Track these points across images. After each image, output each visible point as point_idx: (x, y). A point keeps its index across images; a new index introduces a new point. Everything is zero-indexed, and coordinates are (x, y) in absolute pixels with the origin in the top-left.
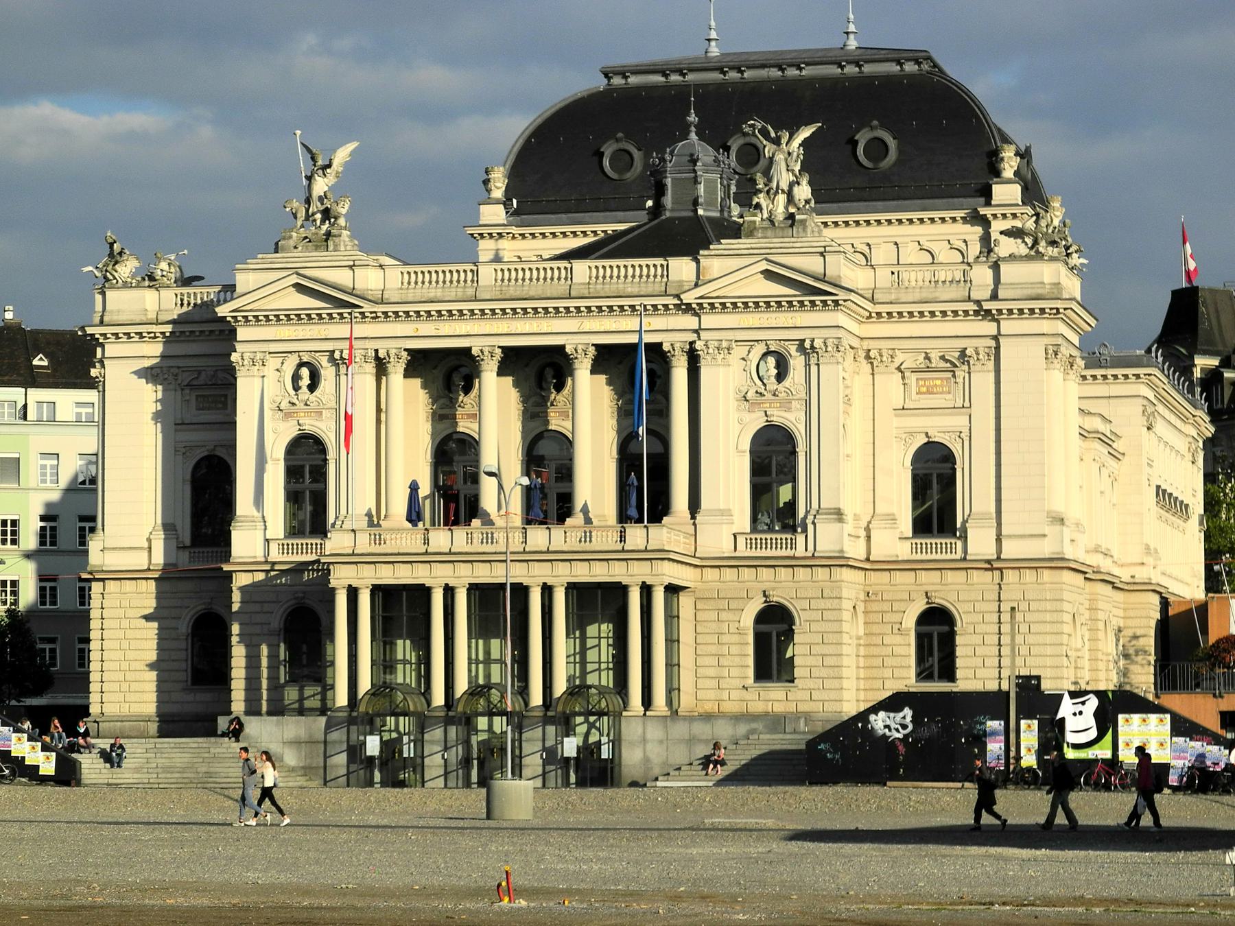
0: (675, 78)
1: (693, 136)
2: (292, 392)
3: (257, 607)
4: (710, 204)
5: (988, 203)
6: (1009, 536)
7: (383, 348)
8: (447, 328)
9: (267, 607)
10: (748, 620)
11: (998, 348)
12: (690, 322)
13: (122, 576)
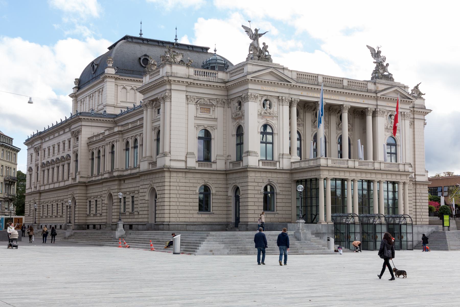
3: (256, 184)
6: (418, 175)
7: (294, 97)
8: (311, 94)
9: (260, 184)
13: (178, 171)
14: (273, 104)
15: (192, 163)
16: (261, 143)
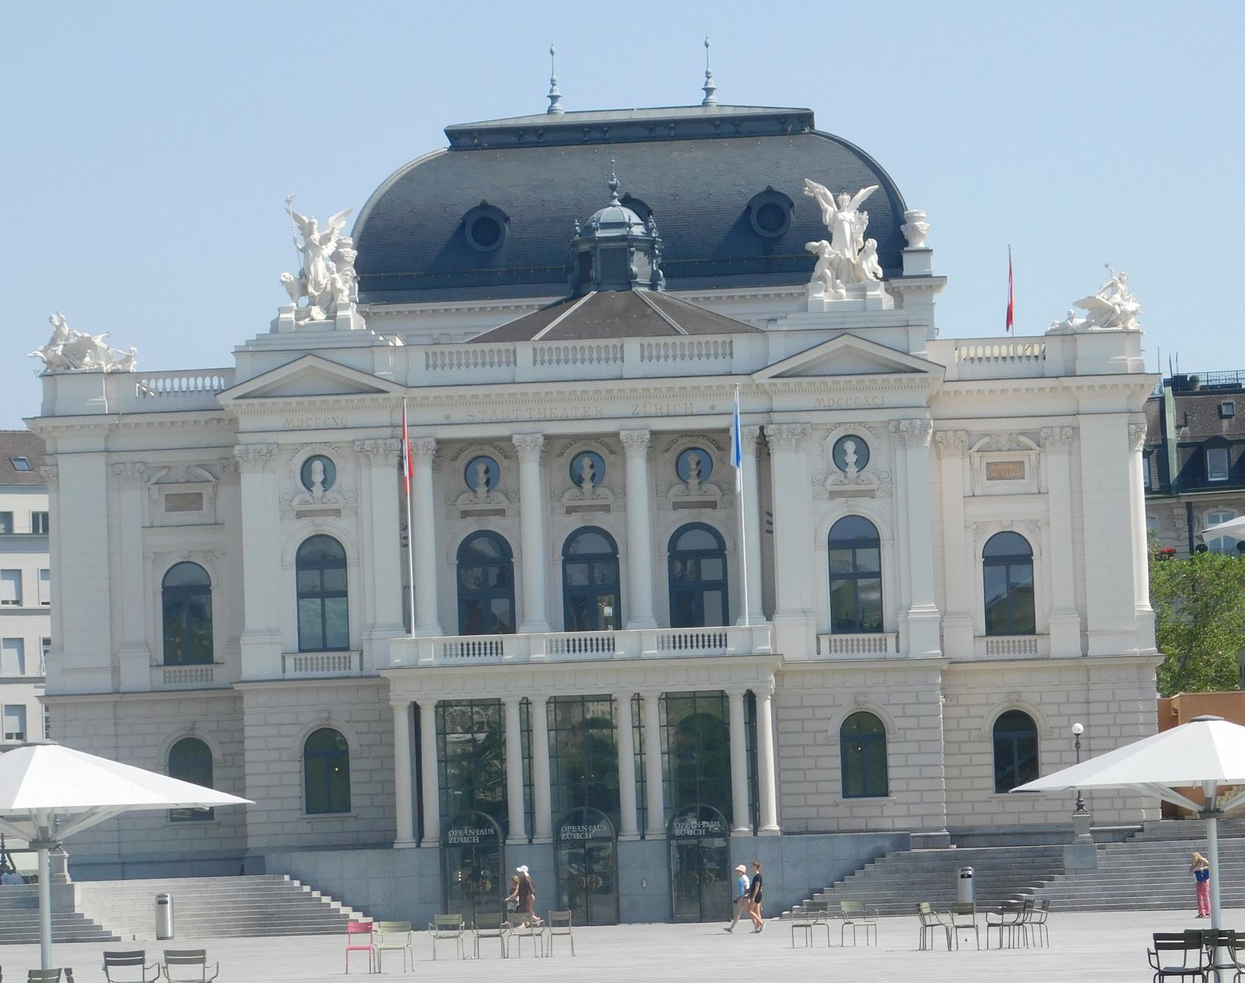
1: (616, 202)
2: (303, 488)
10: (834, 728)
11: (1076, 430)
14: (339, 464)
15: (140, 671)
16: (301, 595)
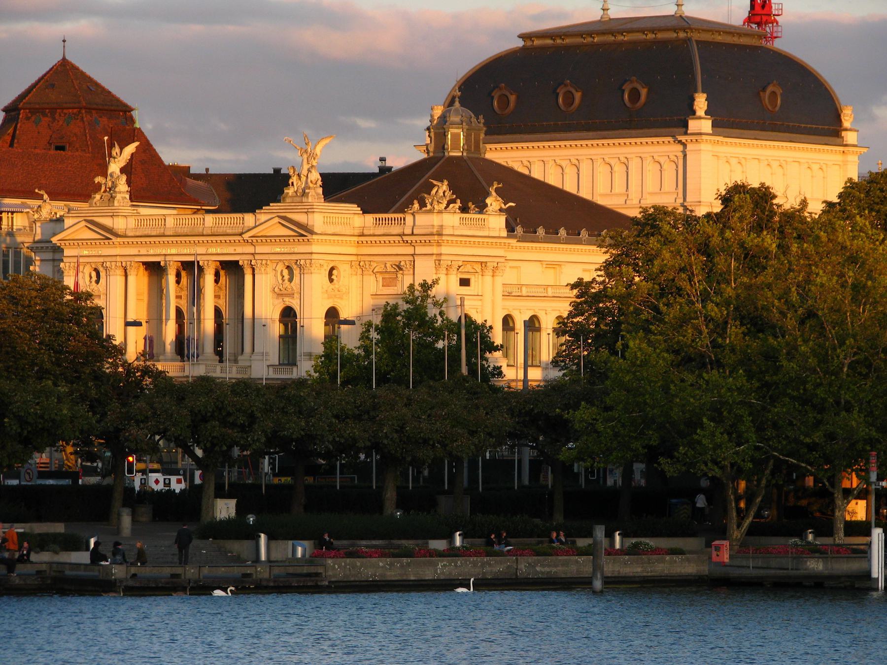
0: (559, 41)
4: (456, 147)
5: (686, 133)
12: (250, 249)
